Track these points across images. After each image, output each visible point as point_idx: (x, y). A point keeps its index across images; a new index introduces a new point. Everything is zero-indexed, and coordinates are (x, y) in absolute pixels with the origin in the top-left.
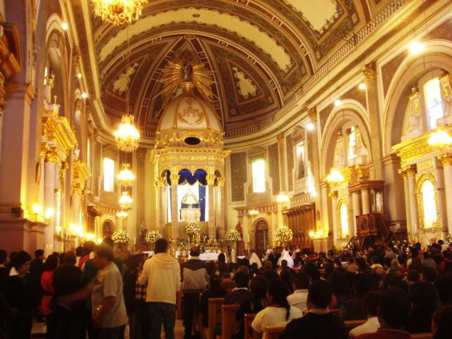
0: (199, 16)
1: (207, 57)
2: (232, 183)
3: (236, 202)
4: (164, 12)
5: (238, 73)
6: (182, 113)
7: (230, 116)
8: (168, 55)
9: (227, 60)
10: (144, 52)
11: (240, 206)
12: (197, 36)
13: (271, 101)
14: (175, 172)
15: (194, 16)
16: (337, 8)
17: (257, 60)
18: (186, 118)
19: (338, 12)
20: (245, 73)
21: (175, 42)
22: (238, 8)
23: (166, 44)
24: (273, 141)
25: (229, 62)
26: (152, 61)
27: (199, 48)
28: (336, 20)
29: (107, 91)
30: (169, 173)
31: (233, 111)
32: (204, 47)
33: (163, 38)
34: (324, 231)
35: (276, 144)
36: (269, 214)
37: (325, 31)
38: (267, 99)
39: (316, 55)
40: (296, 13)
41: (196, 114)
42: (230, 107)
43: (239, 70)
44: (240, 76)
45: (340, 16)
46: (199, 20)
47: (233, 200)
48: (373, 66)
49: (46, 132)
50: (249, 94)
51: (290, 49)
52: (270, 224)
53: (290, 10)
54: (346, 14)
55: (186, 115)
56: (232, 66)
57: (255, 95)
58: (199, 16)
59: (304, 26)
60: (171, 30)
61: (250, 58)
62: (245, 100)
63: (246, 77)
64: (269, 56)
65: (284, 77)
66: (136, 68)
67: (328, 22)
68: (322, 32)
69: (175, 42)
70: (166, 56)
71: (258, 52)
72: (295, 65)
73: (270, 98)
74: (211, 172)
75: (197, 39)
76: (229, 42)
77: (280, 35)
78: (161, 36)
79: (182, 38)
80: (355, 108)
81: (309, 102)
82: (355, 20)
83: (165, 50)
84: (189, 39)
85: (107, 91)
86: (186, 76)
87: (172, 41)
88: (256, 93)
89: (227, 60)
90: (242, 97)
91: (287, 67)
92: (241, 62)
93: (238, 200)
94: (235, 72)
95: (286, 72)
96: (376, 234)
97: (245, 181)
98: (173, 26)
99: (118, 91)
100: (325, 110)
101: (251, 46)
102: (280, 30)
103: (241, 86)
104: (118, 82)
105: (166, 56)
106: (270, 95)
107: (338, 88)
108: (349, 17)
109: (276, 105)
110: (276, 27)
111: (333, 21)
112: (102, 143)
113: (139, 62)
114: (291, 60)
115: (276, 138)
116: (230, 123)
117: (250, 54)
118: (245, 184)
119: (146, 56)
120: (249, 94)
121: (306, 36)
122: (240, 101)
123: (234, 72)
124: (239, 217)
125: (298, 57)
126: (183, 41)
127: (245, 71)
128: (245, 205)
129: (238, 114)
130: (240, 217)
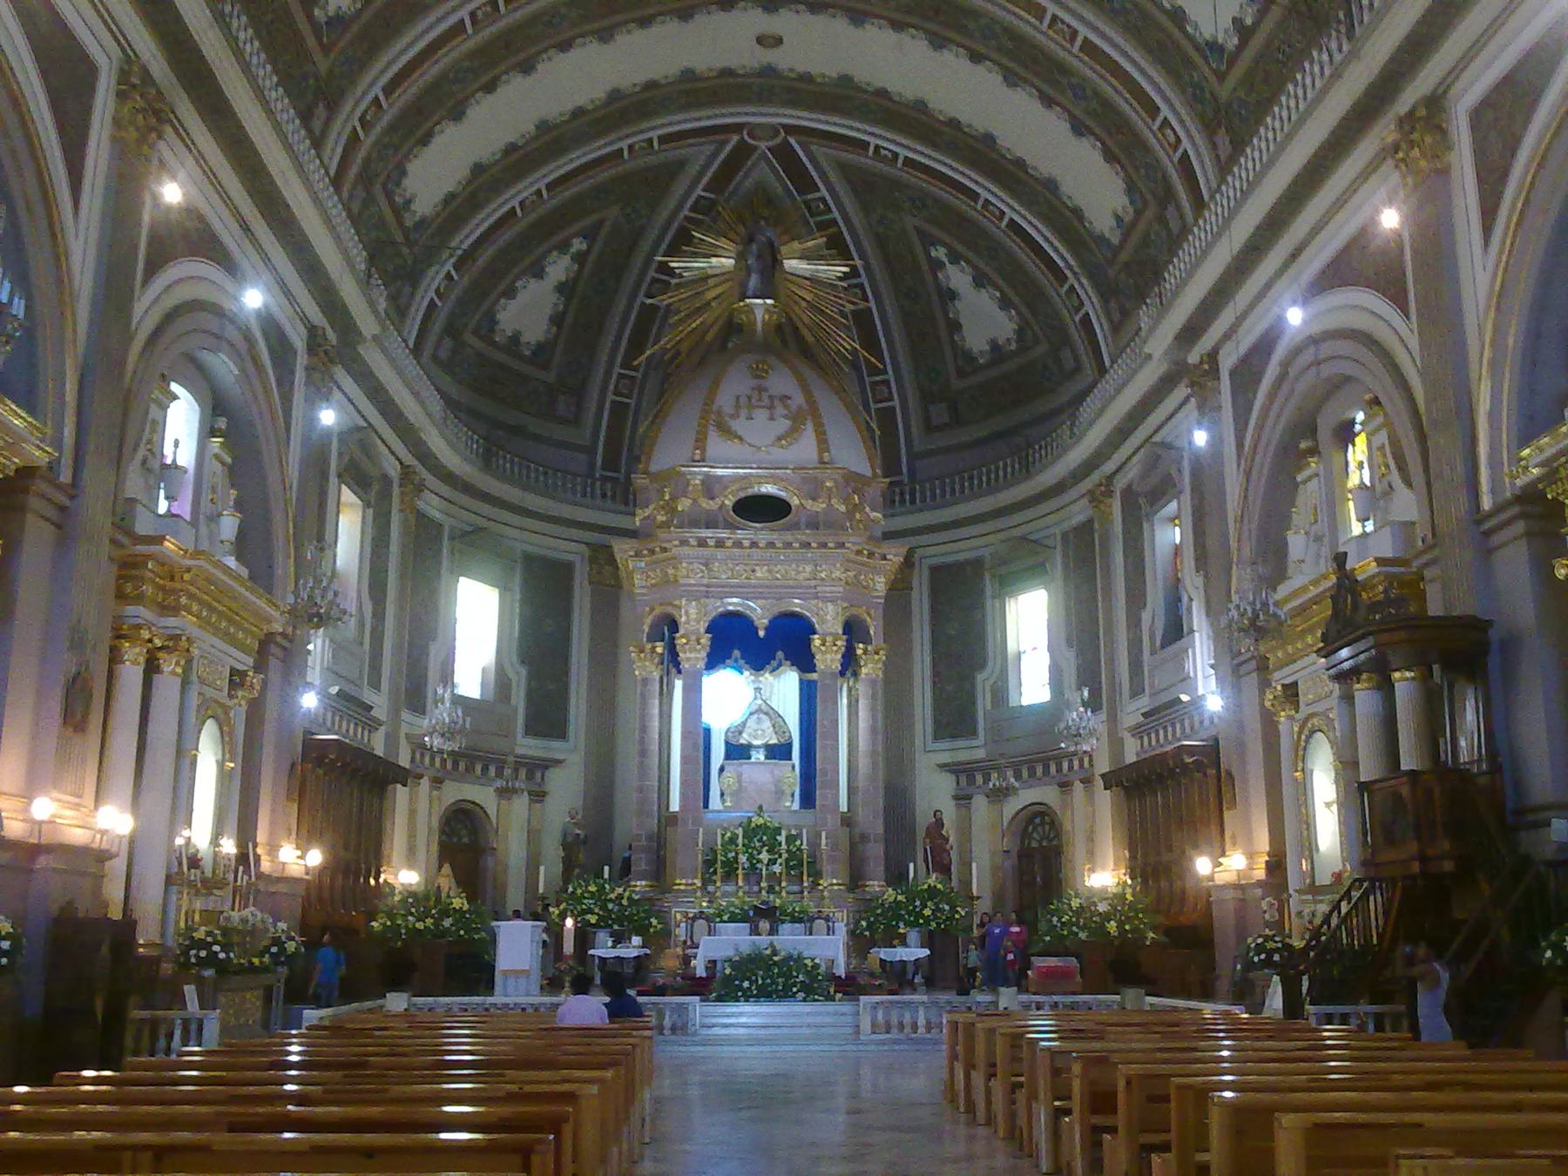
0: (779, 41)
2: (936, 674)
3: (946, 744)
5: (951, 269)
7: (929, 428)
9: (910, 222)
11: (963, 756)
12: (790, 129)
15: (761, 40)
17: (1014, 211)
18: (738, 425)
20: (975, 268)
21: (714, 155)
23: (681, 164)
24: (1079, 513)
25: (915, 227)
26: (639, 233)
27: (803, 182)
29: (470, 338)
30: (674, 626)
31: (940, 413)
32: (823, 175)
33: (663, 139)
34: (1251, 856)
36: (1065, 786)
39: (1214, 146)
41: (780, 410)
42: (927, 398)
43: (955, 258)
44: (958, 278)
47: (936, 738)
50: (995, 346)
52: (1067, 826)
55: (744, 413)
56: (929, 241)
58: (779, 41)
63: (980, 281)
64: (1051, 185)
66: (580, 258)
69: (714, 155)
72: (1145, 204)
74: (828, 621)
75: (792, 141)
77: (1080, 90)
79: (735, 138)
80: (1362, 322)
81: (1191, 332)
83: (679, 189)
84: (763, 145)
85: (470, 338)
90: (969, 357)
91: (1119, 219)
93: (954, 737)
94: (941, 265)
95: (1115, 241)
96: (1448, 866)
100: (1245, 361)
106: (1066, 340)
107: (1294, 256)
109: (1089, 371)
113: (589, 235)
114: (1131, 189)
115: (1085, 501)
116: (930, 453)
117: (987, 190)
118: (980, 677)
119: (613, 212)
120: (995, 346)
122: (961, 373)
123: (937, 265)
124: (956, 798)
125: (1154, 169)
126: (743, 151)
128: (981, 754)
129: (957, 421)
130: (962, 799)
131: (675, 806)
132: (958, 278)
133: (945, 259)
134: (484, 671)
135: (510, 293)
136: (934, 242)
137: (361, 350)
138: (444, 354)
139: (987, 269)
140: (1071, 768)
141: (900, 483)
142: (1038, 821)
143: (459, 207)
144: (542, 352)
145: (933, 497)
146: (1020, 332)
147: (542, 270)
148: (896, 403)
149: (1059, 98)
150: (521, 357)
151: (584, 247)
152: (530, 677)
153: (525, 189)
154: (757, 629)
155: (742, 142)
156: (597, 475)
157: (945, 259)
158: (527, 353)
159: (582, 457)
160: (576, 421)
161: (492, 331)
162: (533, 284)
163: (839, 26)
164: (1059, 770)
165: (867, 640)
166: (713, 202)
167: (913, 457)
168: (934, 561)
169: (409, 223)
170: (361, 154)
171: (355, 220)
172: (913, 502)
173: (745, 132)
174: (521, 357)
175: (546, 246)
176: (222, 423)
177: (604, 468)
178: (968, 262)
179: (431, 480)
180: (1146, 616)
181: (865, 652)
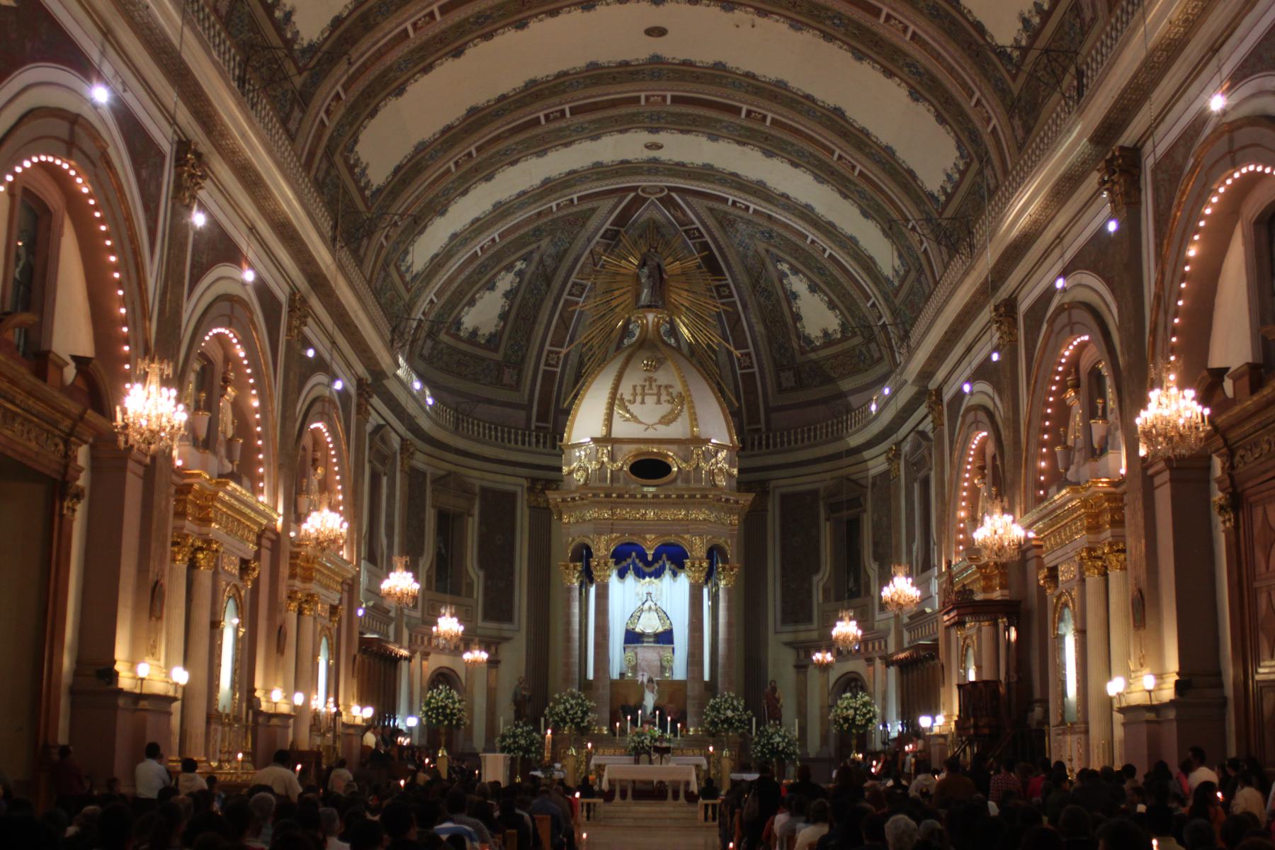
1: (708, 238)
2: (784, 576)
4: (566, 145)
5: (793, 278)
6: (627, 396)
7: (781, 389)
10: (538, 233)
12: (671, 189)
13: (876, 355)
14: (602, 547)
15: (648, 147)
16: (959, 148)
19: (962, 156)
20: (809, 278)
22: (750, 130)
28: (963, 174)
30: (590, 554)
31: (788, 378)
33: (580, 199)
37: (949, 197)
38: (869, 350)
40: (878, 146)
41: (664, 397)
42: (779, 368)
43: (795, 271)
44: (798, 284)
46: (662, 155)
48: (1009, 307)
50: (826, 333)
51: (891, 229)
53: (868, 141)
59: (906, 180)
60: (598, 179)
62: (815, 349)
63: (813, 288)
65: (895, 297)
66: (520, 274)
67: (949, 177)
68: (943, 198)
71: (828, 229)
73: (873, 346)
75: (674, 195)
79: (632, 195)
83: (592, 224)
84: (653, 198)
85: (443, 337)
86: (645, 295)
87: (607, 204)
88: (843, 332)
89: (761, 246)
90: (808, 340)
92: (796, 251)
95: (896, 283)
99: (474, 333)
102: (857, 181)
103: (803, 313)
104: (473, 310)
107: (969, 349)
110: (847, 175)
111: (956, 176)
112: (429, 471)
113: (525, 258)
114: (900, 256)
115: (883, 458)
119: (545, 243)
123: (783, 275)
127: (809, 274)
131: (591, 676)
132: (798, 284)
133: (788, 272)
135: (472, 303)
136: (779, 260)
137: (385, 382)
138: (426, 352)
139: (817, 280)
140: (874, 648)
141: (758, 431)
142: (853, 684)
143: (438, 262)
144: (493, 340)
145: (782, 443)
146: (843, 326)
147: (494, 284)
148: (756, 369)
149: (851, 195)
150: (478, 345)
152: (487, 578)
153: (484, 240)
154: (646, 555)
155: (637, 196)
156: (533, 427)
157: (788, 272)
158: (483, 342)
159: (522, 414)
160: (517, 387)
161: (459, 329)
162: (488, 295)
163: (703, 140)
164: (866, 649)
165: (725, 561)
166: (618, 232)
167: (768, 410)
168: (784, 490)
169: (408, 278)
172: (768, 446)
173: (639, 191)
174: (478, 345)
175: (496, 269)
177: (537, 420)
178: (805, 275)
179: (419, 444)
180: (915, 548)
181: (724, 569)
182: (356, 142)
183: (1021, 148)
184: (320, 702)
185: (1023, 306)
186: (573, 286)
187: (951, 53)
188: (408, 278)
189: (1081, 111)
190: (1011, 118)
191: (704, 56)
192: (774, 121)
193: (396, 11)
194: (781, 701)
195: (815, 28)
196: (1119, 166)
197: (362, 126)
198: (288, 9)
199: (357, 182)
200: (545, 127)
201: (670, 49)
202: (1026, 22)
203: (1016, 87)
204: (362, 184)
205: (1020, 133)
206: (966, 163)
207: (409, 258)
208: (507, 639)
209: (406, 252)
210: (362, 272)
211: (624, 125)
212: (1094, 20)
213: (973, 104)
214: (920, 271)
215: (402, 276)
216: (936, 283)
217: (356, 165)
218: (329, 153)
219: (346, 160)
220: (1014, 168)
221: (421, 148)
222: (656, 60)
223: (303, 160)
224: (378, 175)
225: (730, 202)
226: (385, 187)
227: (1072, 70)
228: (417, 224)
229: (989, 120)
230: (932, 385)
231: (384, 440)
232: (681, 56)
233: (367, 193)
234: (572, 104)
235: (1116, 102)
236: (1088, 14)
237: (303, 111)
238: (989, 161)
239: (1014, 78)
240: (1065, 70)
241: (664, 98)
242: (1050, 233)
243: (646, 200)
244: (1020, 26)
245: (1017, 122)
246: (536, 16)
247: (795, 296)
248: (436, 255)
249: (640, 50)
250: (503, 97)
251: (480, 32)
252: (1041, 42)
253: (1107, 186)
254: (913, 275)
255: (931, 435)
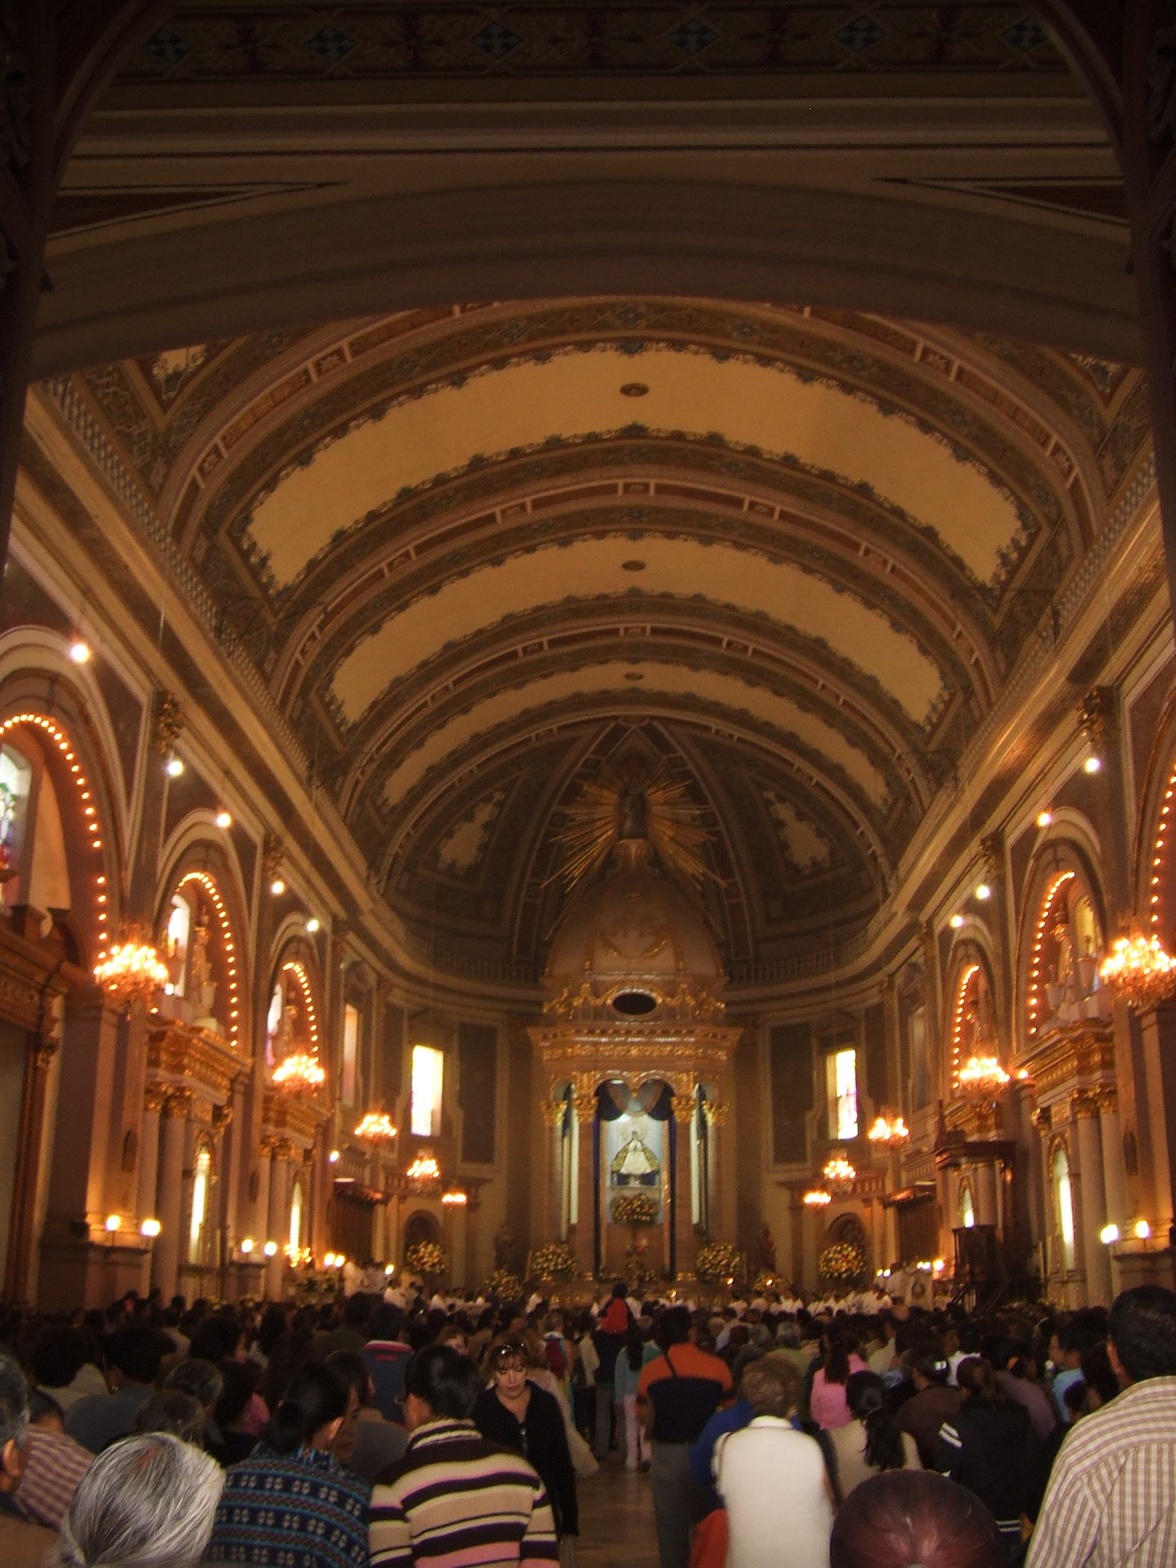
0: (641, 677)
1: (690, 766)
3: (786, 1167)
8: (584, 766)
12: (653, 718)
17: (818, 777)
19: (946, 687)
21: (596, 736)
32: (679, 743)
35: (879, 1007)
37: (935, 727)
43: (782, 799)
44: (784, 812)
45: (953, 696)
46: (644, 685)
48: (995, 844)
49: (164, 1057)
50: (814, 862)
51: (879, 760)
52: (868, 1231)
54: (960, 698)
57: (828, 865)
58: (641, 677)
59: (892, 709)
61: (799, 769)
63: (800, 816)
66: (500, 804)
69: (596, 736)
70: (578, 768)
71: (814, 757)
75: (656, 723)
76: (738, 733)
78: (554, 724)
79: (613, 724)
81: (916, 904)
82: (977, 713)
95: (885, 811)
97: (810, 1107)
98: (578, 701)
99: (453, 864)
101: (790, 740)
105: (578, 768)
108: (966, 702)
111: (941, 707)
114: (888, 785)
117: (799, 762)
118: (809, 1115)
120: (814, 862)
121: (903, 734)
123: (769, 803)
126: (618, 732)
134: (433, 1113)
135: (450, 834)
137: (361, 918)
140: (870, 1188)
143: (414, 796)
144: (472, 871)
146: (832, 853)
151: (503, 796)
155: (617, 725)
163: (684, 671)
164: (863, 1189)
169: (385, 810)
170: (360, 787)
171: (352, 828)
176: (292, 995)
179: (397, 980)
180: (910, 1083)
182: (331, 680)
183: (1004, 679)
184: (295, 1252)
185: (1010, 841)
186: (554, 816)
187: (931, 586)
188: (385, 810)
189: (1057, 652)
190: (993, 651)
191: (683, 588)
192: (755, 652)
193: (372, 551)
194: (775, 1244)
195: (796, 562)
196: (1097, 705)
197: (337, 664)
198: (264, 554)
199: (332, 718)
200: (522, 660)
201: (649, 582)
202: (1004, 557)
203: (997, 621)
204: (338, 721)
205: (1002, 667)
206: (950, 694)
207: (386, 791)
208: (490, 1181)
209: (382, 787)
210: (337, 808)
211: (603, 656)
212: (1070, 558)
213: (955, 636)
214: (908, 799)
215: (378, 809)
216: (925, 812)
217: (330, 703)
218: (304, 693)
219: (322, 697)
220: (998, 699)
221: (397, 683)
222: (634, 592)
223: (278, 702)
224: (354, 711)
225: (713, 731)
226: (361, 723)
227: (1048, 610)
228: (392, 761)
229: (972, 652)
230: (923, 918)
231: (361, 977)
232: (660, 588)
233: (343, 729)
234: (551, 637)
235: (1093, 642)
236: (1064, 552)
237: (278, 653)
238: (972, 693)
239: (995, 611)
240: (1041, 611)
241: (644, 629)
242: (1035, 766)
243: (625, 730)
244: (999, 561)
245: (999, 656)
246: (513, 552)
247: (780, 824)
248: (413, 789)
249: (619, 583)
250: (479, 632)
251: (455, 570)
252: (1017, 583)
253: (1086, 725)
254: (901, 804)
255: (924, 968)
